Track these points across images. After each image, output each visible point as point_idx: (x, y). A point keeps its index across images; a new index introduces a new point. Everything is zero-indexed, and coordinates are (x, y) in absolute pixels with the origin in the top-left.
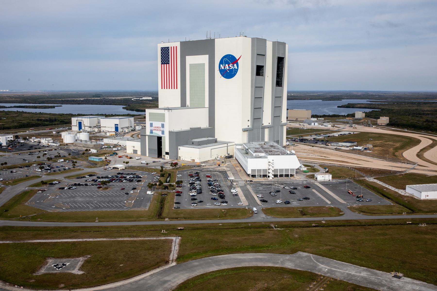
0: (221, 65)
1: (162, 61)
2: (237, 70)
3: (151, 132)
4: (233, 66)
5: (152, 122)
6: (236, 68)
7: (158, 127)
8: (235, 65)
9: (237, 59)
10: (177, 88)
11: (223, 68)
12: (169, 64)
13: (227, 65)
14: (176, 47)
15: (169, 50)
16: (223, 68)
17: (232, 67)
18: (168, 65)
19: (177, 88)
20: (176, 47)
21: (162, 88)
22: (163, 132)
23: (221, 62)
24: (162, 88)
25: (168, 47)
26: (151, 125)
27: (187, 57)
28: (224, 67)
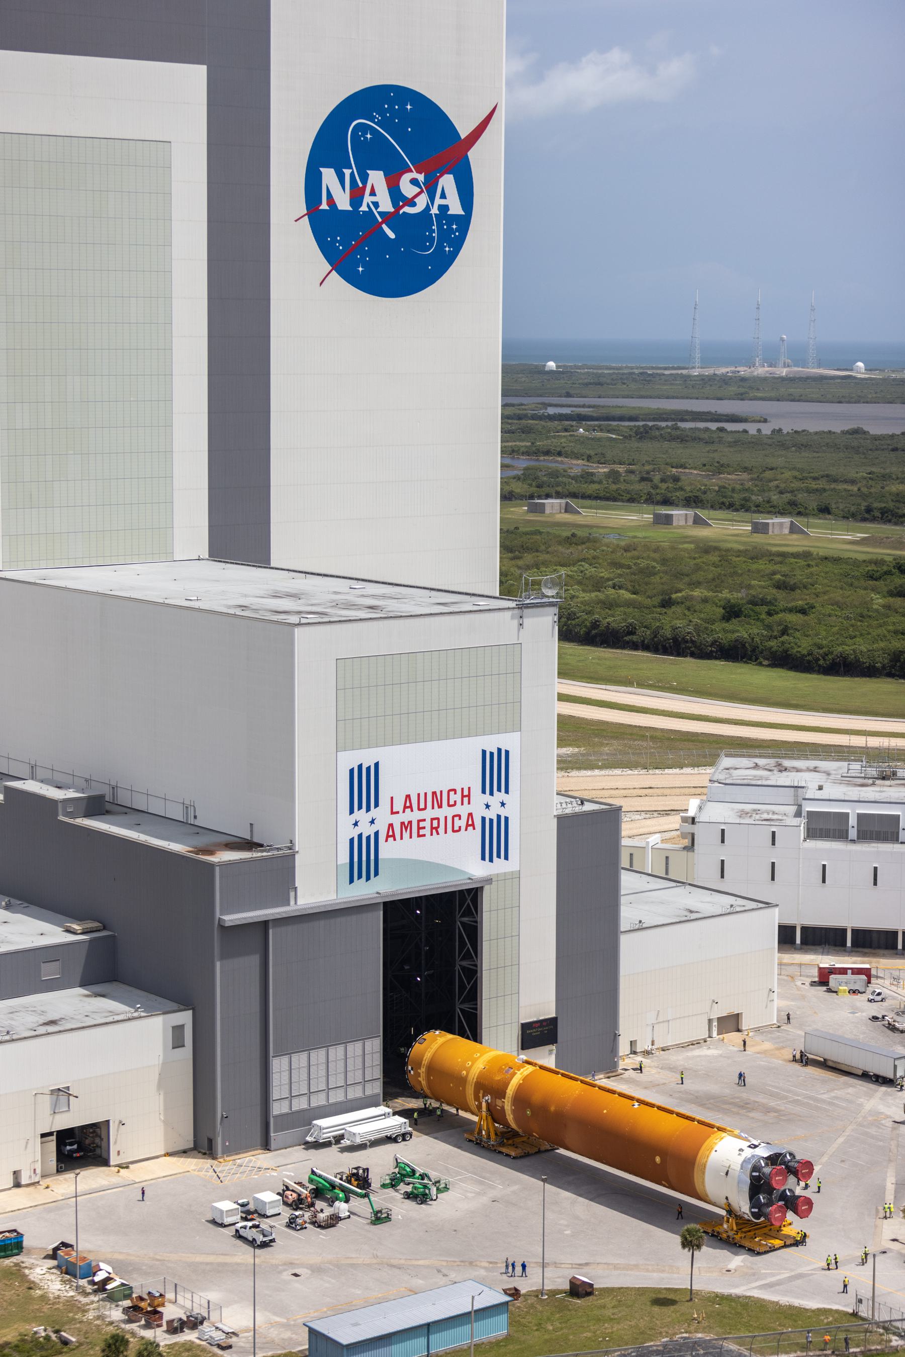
0: (329, 176)
2: (464, 222)
3: (364, 860)
4: (431, 187)
5: (367, 757)
6: (456, 209)
7: (437, 799)
8: (447, 182)
9: (463, 133)
11: (343, 203)
13: (377, 178)
16: (343, 203)
17: (422, 202)
22: (495, 839)
26: (364, 787)
28: (357, 195)
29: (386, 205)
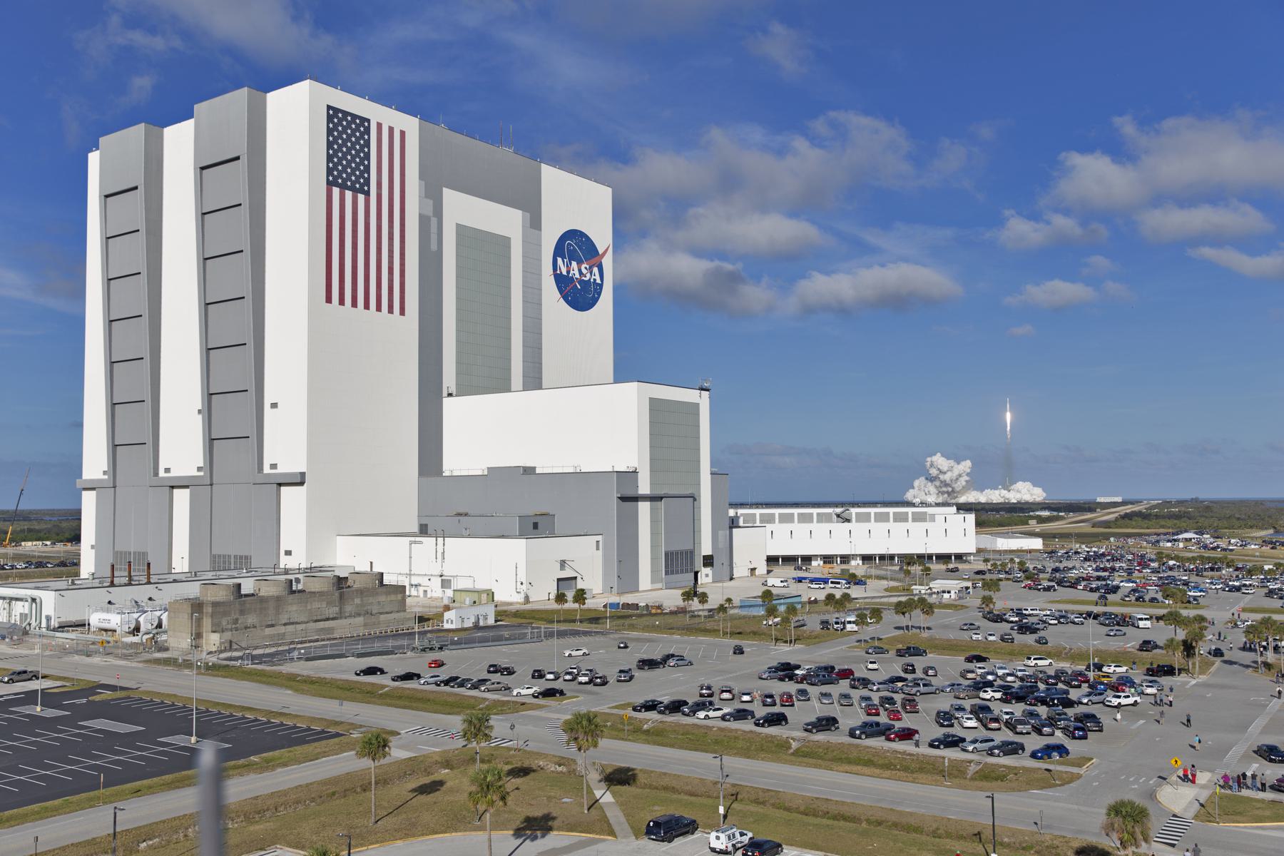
0: (559, 260)
1: (329, 172)
2: (601, 286)
6: (599, 281)
8: (596, 270)
10: (402, 312)
11: (564, 273)
12: (367, 194)
13: (574, 264)
14: (403, 133)
15: (368, 131)
16: (564, 273)
18: (361, 197)
19: (402, 312)
20: (403, 133)
21: (329, 300)
23: (559, 251)
24: (329, 300)
25: (364, 120)
27: (445, 190)
29: (577, 276)
